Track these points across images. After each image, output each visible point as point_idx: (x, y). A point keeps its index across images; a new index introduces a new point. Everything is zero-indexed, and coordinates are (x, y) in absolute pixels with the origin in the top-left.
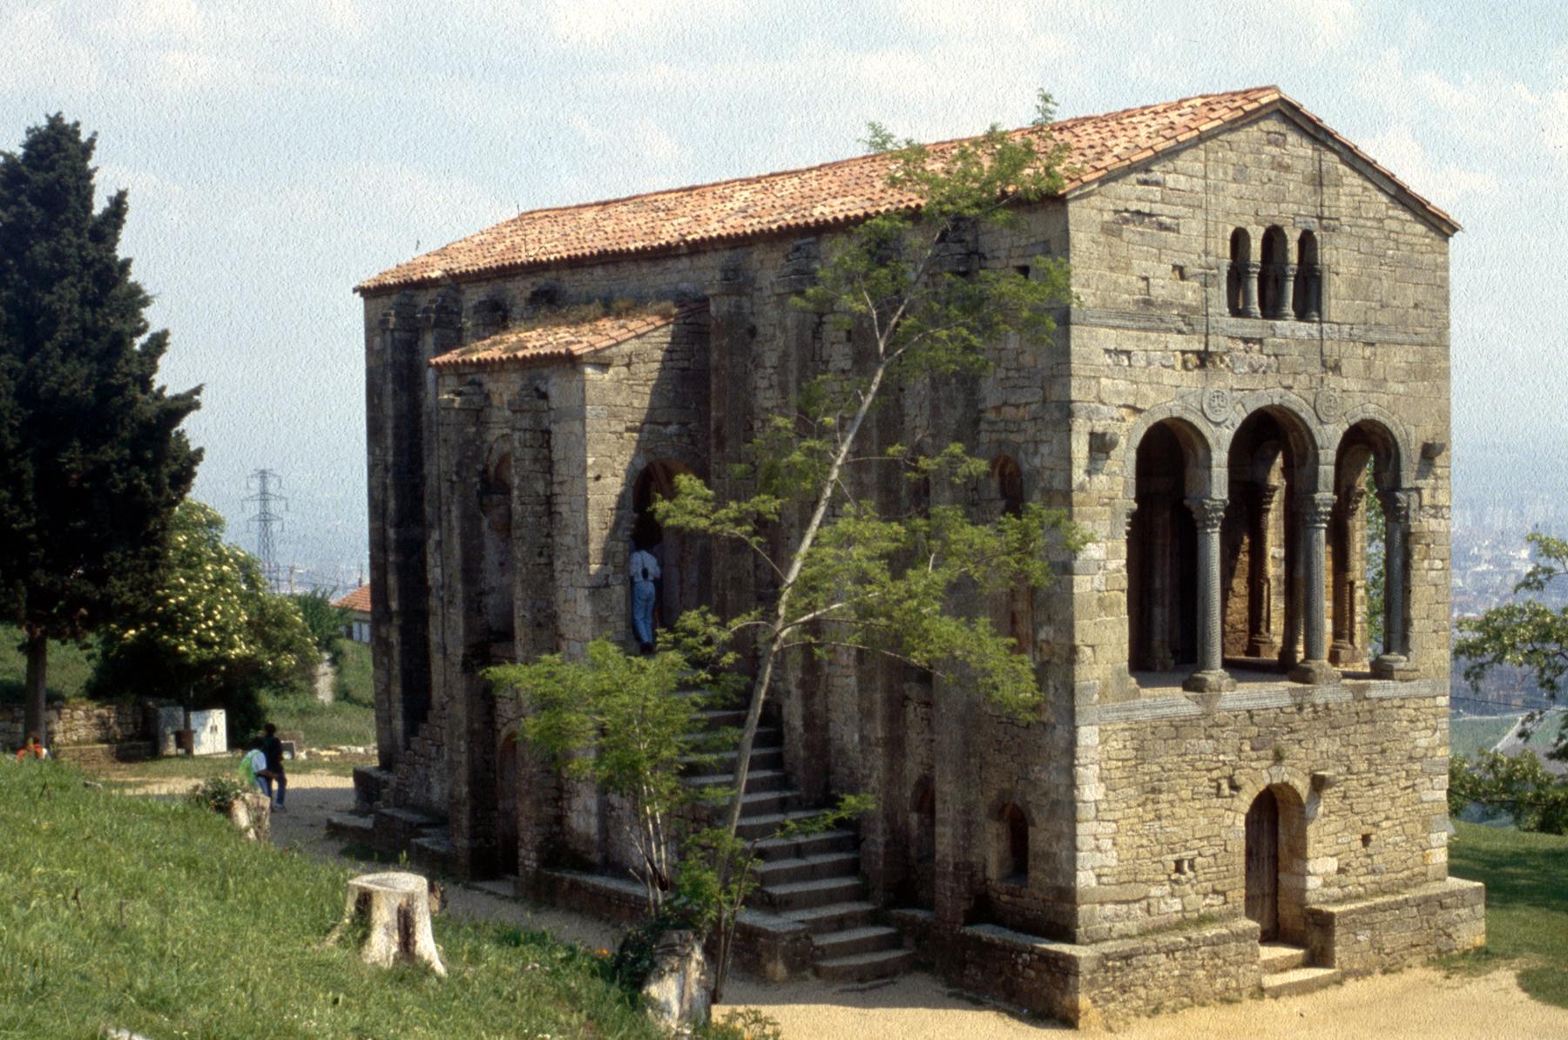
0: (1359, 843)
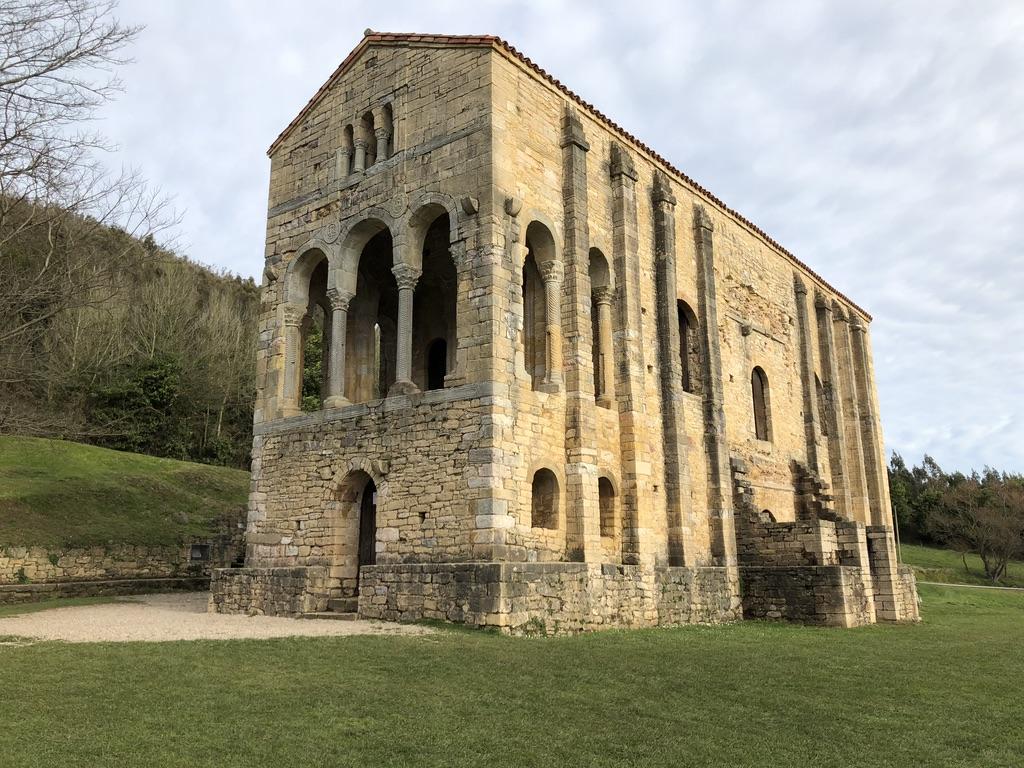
0: (418, 519)
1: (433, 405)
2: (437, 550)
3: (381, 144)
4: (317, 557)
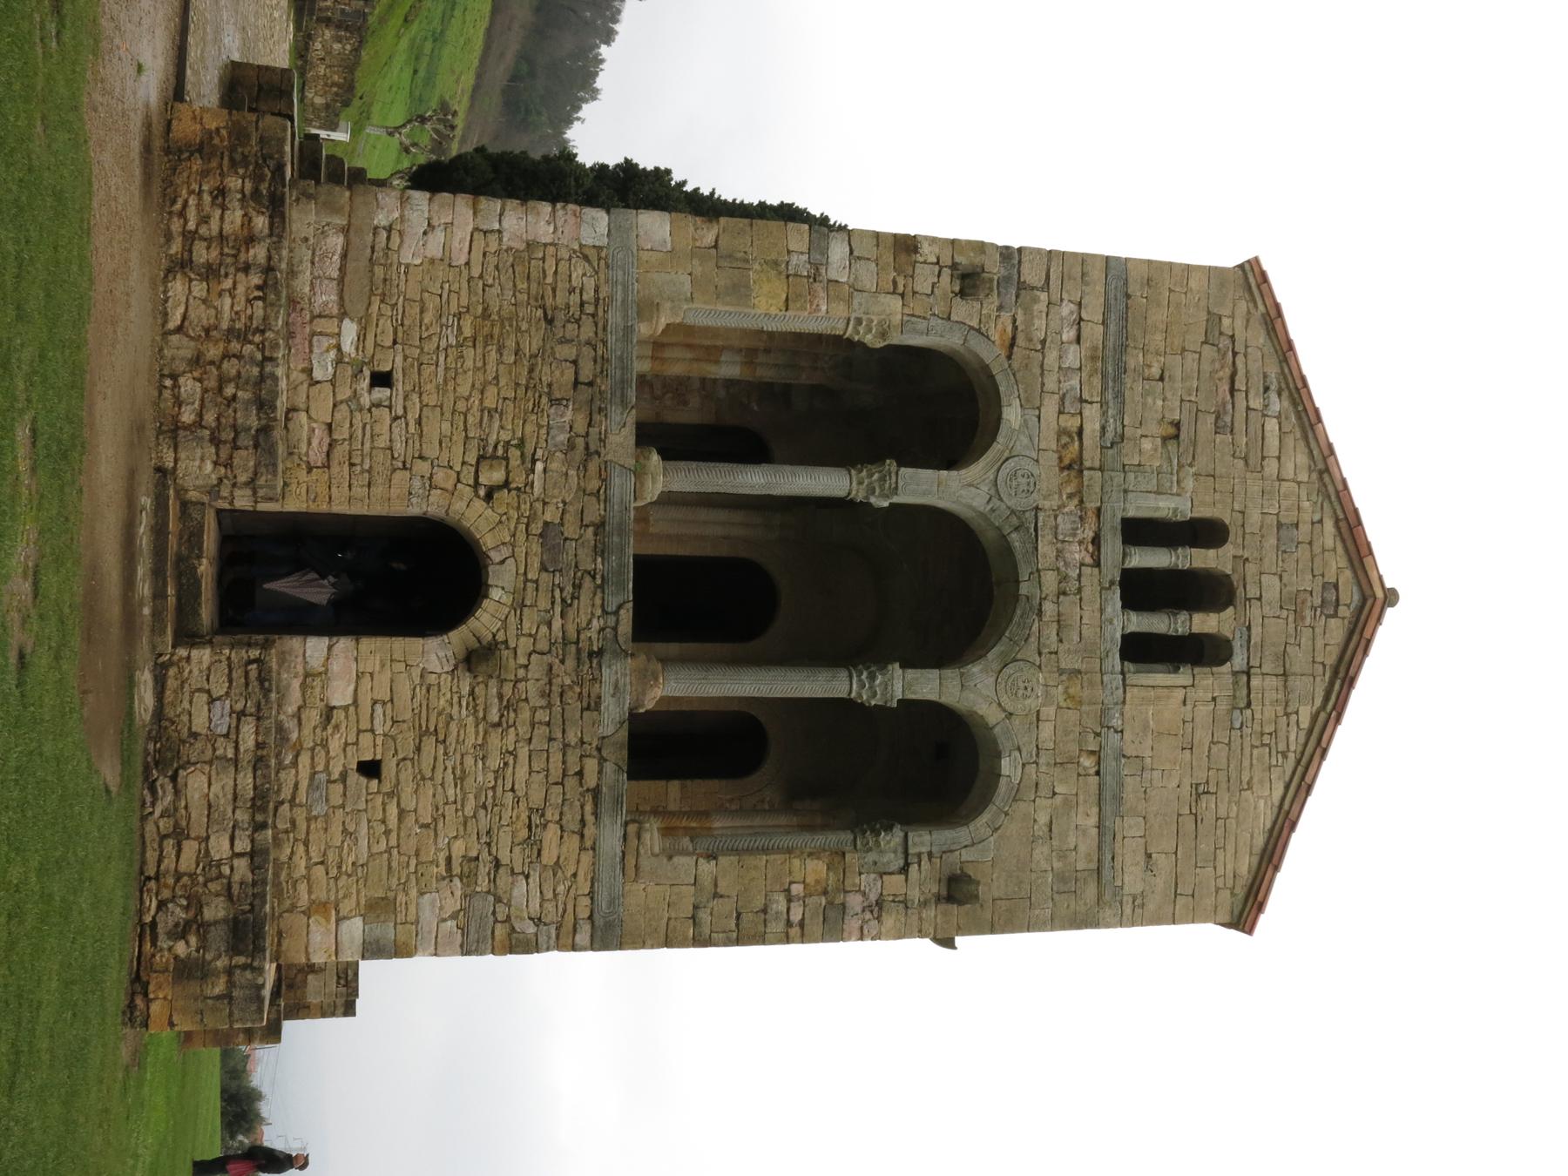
1: (596, 792)
4: (304, 448)
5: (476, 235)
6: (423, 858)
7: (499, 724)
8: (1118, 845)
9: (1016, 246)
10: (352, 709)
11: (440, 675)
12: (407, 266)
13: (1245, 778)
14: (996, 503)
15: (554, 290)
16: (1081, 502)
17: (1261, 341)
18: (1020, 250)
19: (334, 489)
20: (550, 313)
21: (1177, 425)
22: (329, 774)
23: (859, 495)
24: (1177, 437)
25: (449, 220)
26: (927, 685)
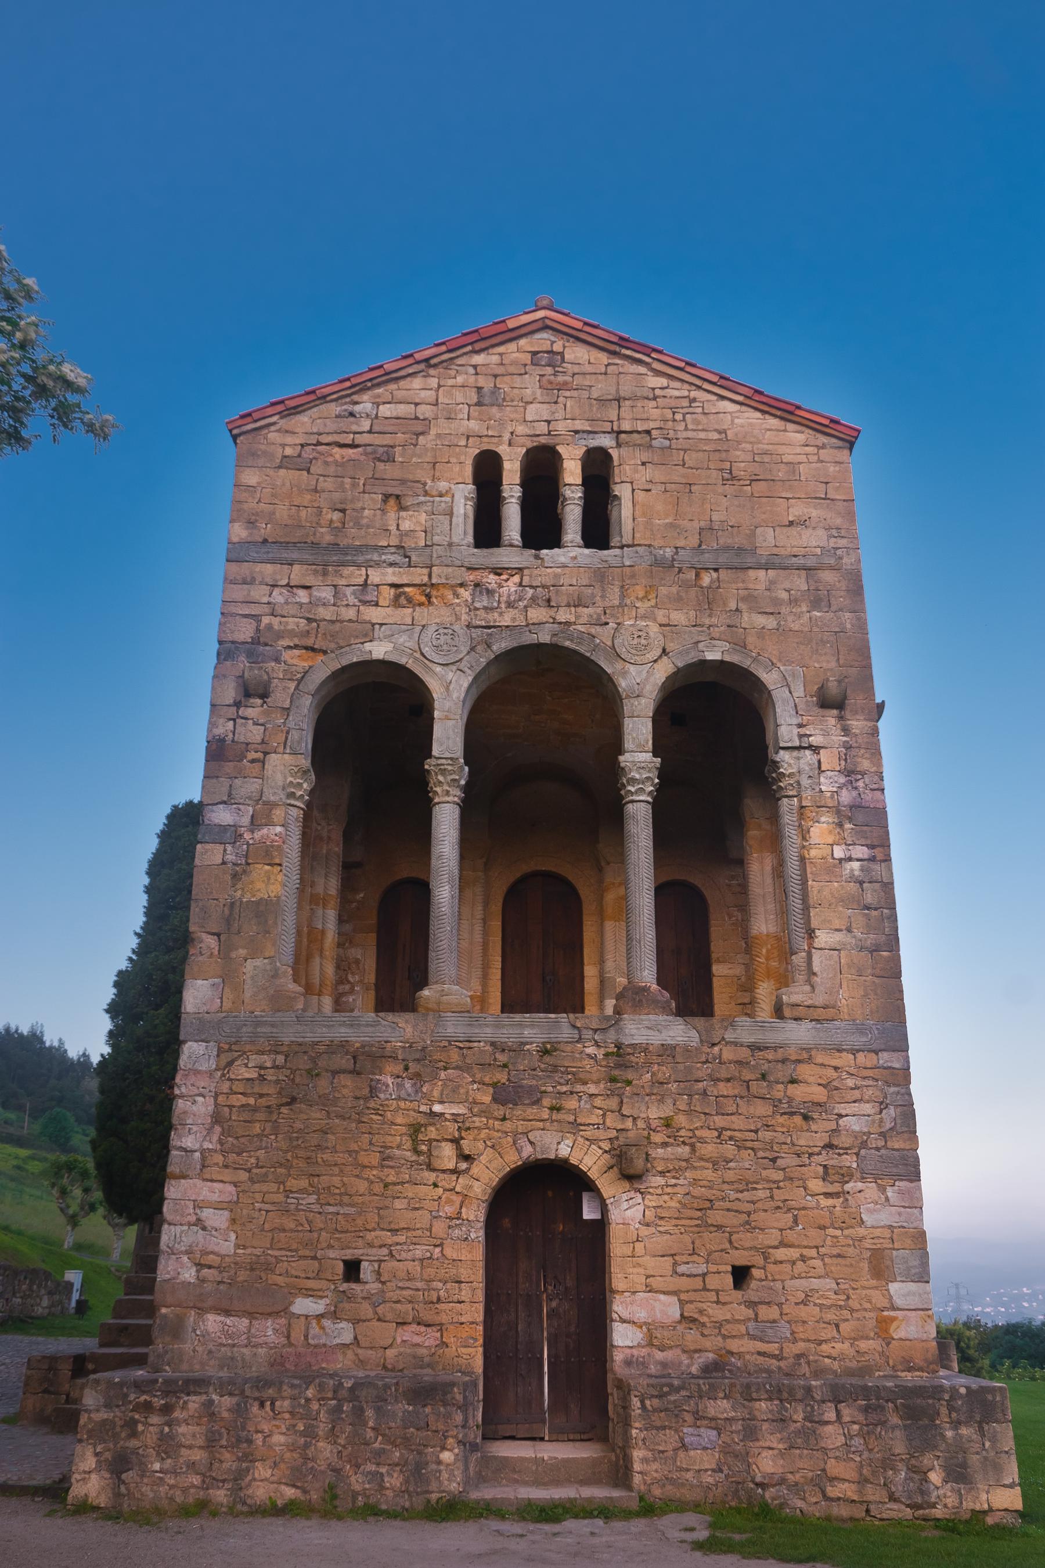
0: (729, 1280)
1: (755, 1048)
2: (792, 1349)
3: (573, 515)
5: (208, 1176)
6: (827, 1222)
7: (693, 1146)
8: (782, 552)
9: (217, 646)
10: (683, 1296)
11: (647, 1207)
12: (237, 1246)
13: (716, 436)
14: (463, 665)
15: (261, 1096)
16: (461, 585)
17: (306, 419)
18: (220, 642)
19: (463, 1320)
20: (284, 1100)
21: (386, 497)
22: (749, 1319)
23: (456, 794)
24: (398, 497)
25: (191, 1204)
26: (638, 731)
